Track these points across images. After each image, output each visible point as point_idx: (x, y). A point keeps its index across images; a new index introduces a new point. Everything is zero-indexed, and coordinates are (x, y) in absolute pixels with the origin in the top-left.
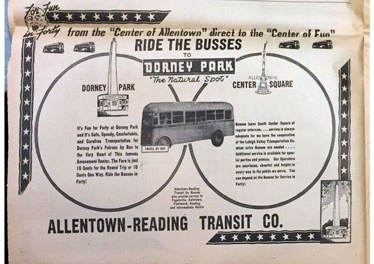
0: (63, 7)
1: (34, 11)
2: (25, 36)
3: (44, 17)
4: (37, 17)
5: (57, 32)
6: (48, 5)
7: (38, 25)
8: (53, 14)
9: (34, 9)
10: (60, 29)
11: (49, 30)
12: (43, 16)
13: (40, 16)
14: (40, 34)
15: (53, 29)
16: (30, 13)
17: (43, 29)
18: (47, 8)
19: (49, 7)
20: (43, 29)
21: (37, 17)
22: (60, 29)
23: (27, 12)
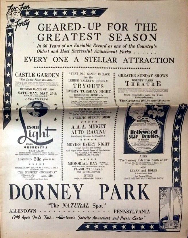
0: (34, 6)
1: (13, 9)
2: (7, 28)
3: (19, 13)
4: (15, 13)
5: (28, 24)
6: (22, 5)
7: (15, 19)
8: (25, 11)
9: (14, 8)
10: (29, 22)
11: (22, 22)
12: (19, 12)
13: (16, 13)
14: (17, 26)
15: (25, 22)
16: (10, 10)
17: (18, 22)
18: (22, 7)
19: (23, 6)
20: (18, 22)
21: (15, 13)
22: (29, 22)
23: (9, 10)
